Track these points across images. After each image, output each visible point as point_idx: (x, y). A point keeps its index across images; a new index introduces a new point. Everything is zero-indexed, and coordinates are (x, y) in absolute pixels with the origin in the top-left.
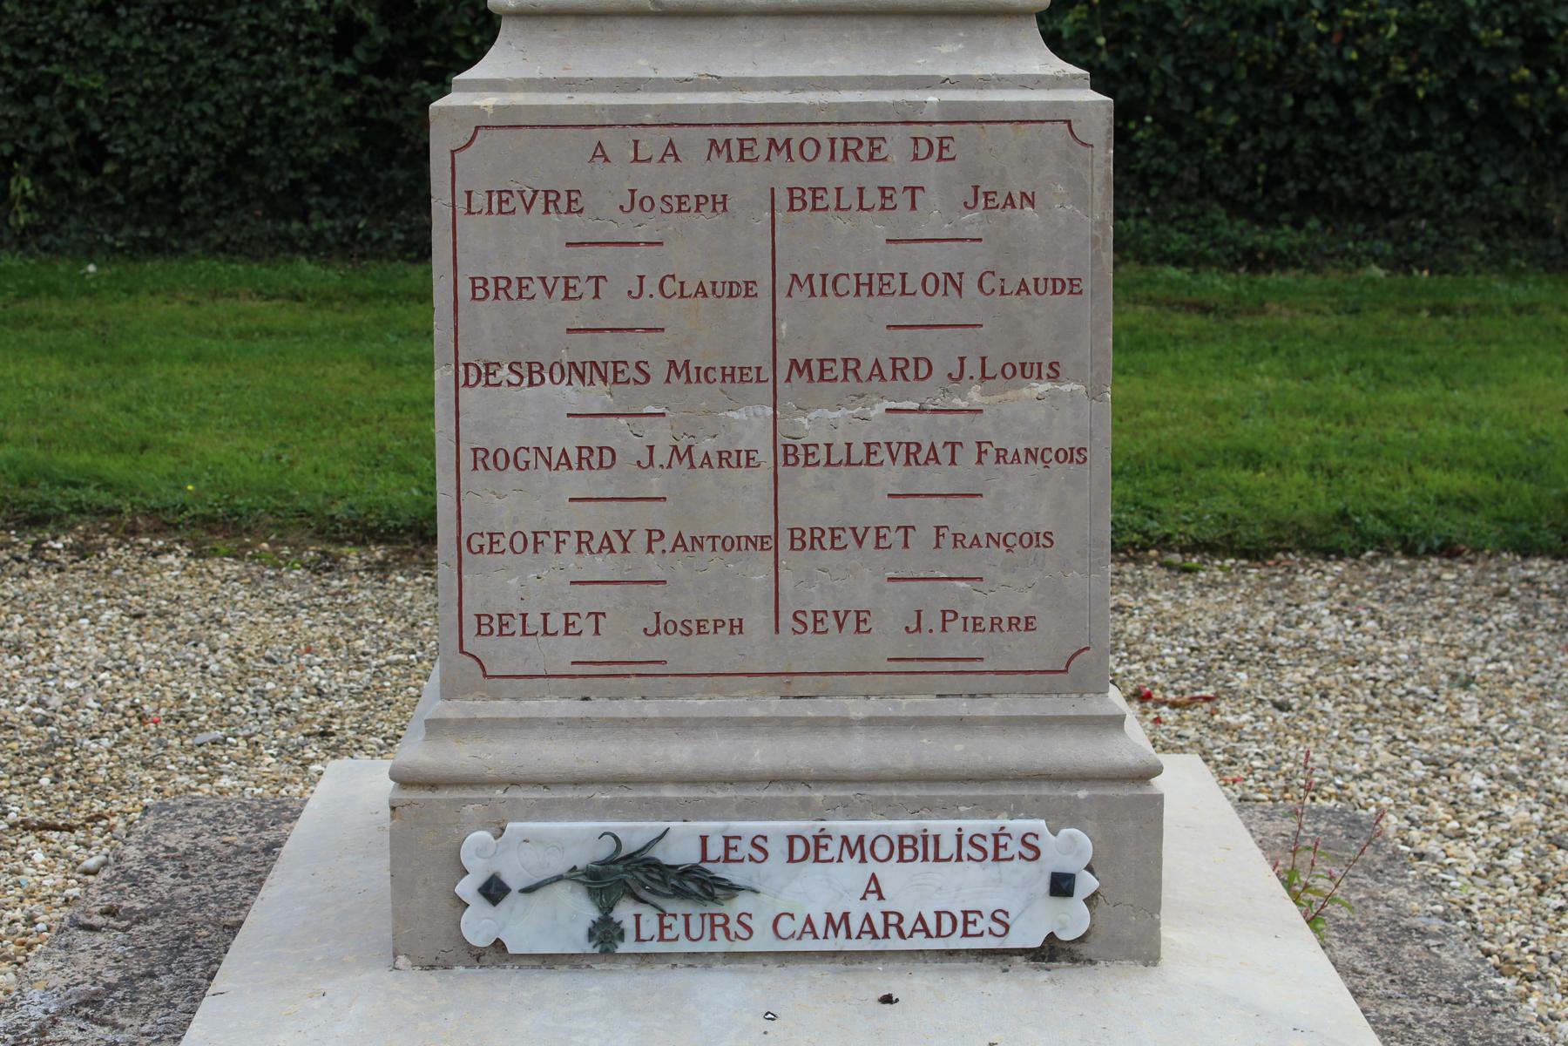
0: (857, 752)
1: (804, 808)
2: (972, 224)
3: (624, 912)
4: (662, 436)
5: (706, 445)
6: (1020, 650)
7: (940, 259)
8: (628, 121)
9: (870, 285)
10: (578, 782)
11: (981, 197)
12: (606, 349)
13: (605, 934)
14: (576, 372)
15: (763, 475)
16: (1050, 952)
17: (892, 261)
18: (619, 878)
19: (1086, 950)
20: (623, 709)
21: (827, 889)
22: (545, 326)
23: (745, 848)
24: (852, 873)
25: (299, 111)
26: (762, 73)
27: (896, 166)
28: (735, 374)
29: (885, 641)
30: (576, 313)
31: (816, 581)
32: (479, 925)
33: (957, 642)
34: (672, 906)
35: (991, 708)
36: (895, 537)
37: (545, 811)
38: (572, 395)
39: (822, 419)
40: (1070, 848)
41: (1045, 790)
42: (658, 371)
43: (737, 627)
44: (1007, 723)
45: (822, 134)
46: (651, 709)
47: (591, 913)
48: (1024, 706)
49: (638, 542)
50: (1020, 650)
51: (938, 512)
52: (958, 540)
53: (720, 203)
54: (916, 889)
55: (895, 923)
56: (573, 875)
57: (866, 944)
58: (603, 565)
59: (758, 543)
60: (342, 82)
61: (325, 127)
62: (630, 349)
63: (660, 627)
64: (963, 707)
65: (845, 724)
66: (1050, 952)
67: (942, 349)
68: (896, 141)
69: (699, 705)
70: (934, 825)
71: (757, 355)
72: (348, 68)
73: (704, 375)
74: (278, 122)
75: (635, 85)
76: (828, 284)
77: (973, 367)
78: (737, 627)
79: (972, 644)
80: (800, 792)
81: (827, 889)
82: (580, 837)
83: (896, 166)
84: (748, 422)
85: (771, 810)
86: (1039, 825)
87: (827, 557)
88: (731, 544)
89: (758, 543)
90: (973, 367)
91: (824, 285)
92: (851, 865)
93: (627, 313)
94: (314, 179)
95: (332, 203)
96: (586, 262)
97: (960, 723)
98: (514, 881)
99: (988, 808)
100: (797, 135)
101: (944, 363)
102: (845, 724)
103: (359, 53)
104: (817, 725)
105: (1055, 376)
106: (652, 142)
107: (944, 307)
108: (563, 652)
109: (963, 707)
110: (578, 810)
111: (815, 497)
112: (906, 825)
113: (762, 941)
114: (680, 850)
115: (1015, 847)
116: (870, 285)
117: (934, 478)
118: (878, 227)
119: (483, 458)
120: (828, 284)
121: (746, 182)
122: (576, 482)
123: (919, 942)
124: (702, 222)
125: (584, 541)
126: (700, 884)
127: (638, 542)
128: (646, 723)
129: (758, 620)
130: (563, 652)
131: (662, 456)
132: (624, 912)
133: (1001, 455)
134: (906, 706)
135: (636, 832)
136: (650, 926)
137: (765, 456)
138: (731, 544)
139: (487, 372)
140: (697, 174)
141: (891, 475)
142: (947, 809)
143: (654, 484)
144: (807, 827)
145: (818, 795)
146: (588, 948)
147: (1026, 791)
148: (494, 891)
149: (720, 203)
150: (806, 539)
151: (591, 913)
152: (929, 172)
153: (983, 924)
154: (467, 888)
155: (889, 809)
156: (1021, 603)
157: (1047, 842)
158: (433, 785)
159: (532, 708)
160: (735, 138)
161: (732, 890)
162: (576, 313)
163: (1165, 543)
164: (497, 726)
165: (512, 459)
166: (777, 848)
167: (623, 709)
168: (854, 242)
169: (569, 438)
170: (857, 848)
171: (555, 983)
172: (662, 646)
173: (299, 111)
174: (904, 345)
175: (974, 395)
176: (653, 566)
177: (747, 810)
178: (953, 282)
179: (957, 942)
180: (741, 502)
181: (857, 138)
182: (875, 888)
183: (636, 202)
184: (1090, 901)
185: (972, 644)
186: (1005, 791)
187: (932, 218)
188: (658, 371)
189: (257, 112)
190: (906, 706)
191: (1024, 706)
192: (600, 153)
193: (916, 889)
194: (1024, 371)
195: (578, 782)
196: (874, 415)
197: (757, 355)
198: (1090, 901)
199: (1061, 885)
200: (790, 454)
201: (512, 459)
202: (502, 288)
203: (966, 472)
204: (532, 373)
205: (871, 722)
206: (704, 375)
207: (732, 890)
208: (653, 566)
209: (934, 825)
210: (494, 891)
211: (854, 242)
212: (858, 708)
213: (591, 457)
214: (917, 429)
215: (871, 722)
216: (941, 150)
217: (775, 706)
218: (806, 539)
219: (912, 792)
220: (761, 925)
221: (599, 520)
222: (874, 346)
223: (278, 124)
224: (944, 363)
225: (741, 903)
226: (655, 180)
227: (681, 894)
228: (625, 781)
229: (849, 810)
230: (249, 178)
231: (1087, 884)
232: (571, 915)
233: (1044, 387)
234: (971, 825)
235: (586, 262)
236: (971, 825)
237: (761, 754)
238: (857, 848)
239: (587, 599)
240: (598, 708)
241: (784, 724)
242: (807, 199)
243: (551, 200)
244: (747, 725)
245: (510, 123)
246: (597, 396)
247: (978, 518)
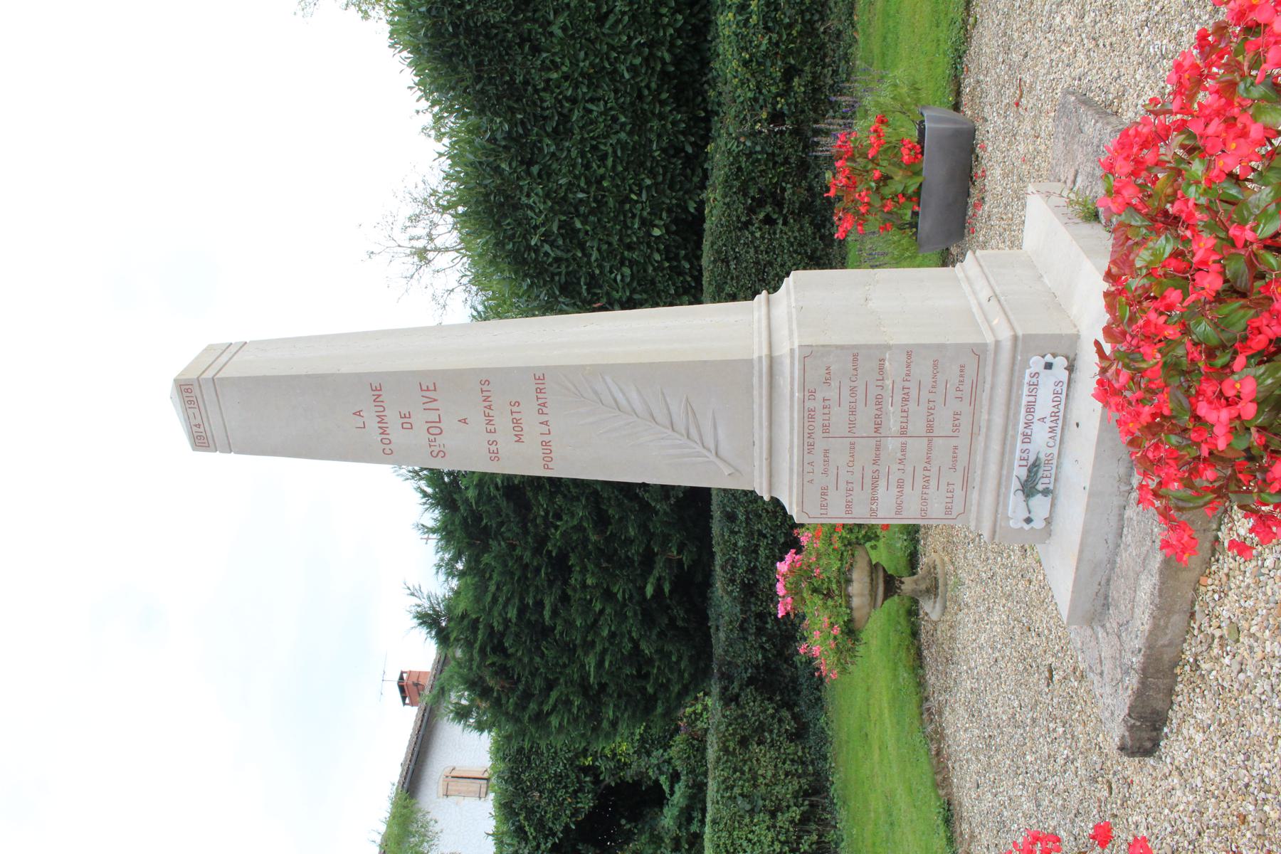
0: (998, 420)
1: (1014, 437)
2: (834, 384)
3: (1040, 487)
4: (895, 467)
5: (899, 455)
6: (970, 372)
7: (846, 392)
8: (802, 474)
9: (853, 412)
10: (998, 496)
11: (827, 382)
12: (868, 481)
13: (1046, 492)
14: (874, 487)
15: (909, 440)
16: (1071, 368)
17: (846, 406)
18: (1029, 489)
19: (1071, 356)
20: (978, 479)
21: (1041, 434)
23: (1025, 455)
24: (1037, 426)
25: (795, 238)
26: (788, 437)
27: (817, 404)
28: (878, 448)
29: (965, 408)
30: (857, 488)
31: (943, 423)
32: (1038, 524)
33: (967, 387)
34: (1040, 475)
35: (989, 379)
36: (931, 405)
37: (1006, 505)
38: (881, 489)
40: (1036, 363)
41: (1017, 368)
42: (875, 467)
43: (956, 448)
44: (994, 374)
45: (807, 424)
46: (979, 472)
47: (1039, 496)
48: (989, 369)
49: (927, 473)
50: (970, 372)
51: (924, 393)
52: (933, 387)
53: (826, 451)
54: (1044, 406)
55: (1054, 414)
56: (1026, 501)
57: (1060, 422)
58: (933, 483)
59: (930, 442)
60: (785, 223)
61: (801, 229)
62: (868, 474)
64: (988, 386)
65: (989, 421)
66: (1071, 368)
67: (873, 391)
68: (809, 404)
69: (979, 458)
70: (1024, 402)
71: (873, 441)
72: (780, 222)
73: (877, 456)
74: (800, 245)
75: (791, 470)
76: (852, 424)
77: (879, 383)
78: (956, 448)
79: (968, 382)
80: (1009, 437)
81: (1041, 434)
82: (1015, 501)
83: (817, 404)
84: (892, 445)
85: (1014, 446)
86: (1028, 372)
87: (936, 423)
88: (930, 449)
89: (930, 442)
90: (879, 383)
92: (1033, 426)
93: (858, 475)
94: (819, 230)
95: (828, 225)
96: (842, 485)
97: (992, 388)
98: (1027, 515)
99: (1020, 385)
100: (807, 431)
102: (989, 421)
103: (775, 216)
104: (988, 428)
105: (883, 360)
106: (808, 468)
108: (959, 493)
109: (988, 386)
110: (1007, 496)
111: (917, 425)
112: (1023, 411)
113: (1055, 451)
114: (1023, 473)
115: (1034, 380)
116: (853, 412)
117: (914, 393)
118: (835, 409)
120: (852, 424)
121: (820, 445)
122: (908, 489)
123: (1062, 407)
125: (925, 487)
126: (1034, 468)
127: (927, 473)
128: (983, 474)
129: (954, 442)
130: (959, 493)
131: (901, 467)
132: (1040, 487)
133: (908, 375)
134: (985, 402)
135: (1015, 485)
136: (1046, 480)
137: (903, 440)
138: (930, 449)
140: (818, 457)
141: (912, 406)
142: (1019, 397)
143: (909, 469)
144: (1020, 438)
145: (1010, 433)
146: (1050, 497)
147: (1016, 374)
149: (826, 451)
150: (930, 428)
151: (1039, 496)
152: (819, 396)
153: (1058, 388)
154: (1027, 527)
155: (1017, 413)
156: (956, 369)
157: (1033, 370)
158: (994, 532)
159: (975, 502)
160: (808, 446)
161: (1037, 459)
162: (857, 488)
163: (965, 22)
164: (979, 512)
165: (899, 505)
166: (1026, 446)
167: (978, 479)
168: (839, 417)
169: (894, 490)
170: (1028, 424)
171: (1060, 509)
172: (960, 467)
173: (795, 238)
175: (888, 382)
176: (935, 469)
177: (1012, 452)
178: (853, 389)
179: (1064, 396)
180: (917, 448)
181: (808, 415)
182: (1042, 419)
183: (825, 472)
184: (1054, 356)
185: (968, 382)
186: (1016, 380)
187: (833, 395)
188: (875, 467)
189: (795, 251)
190: (985, 402)
191: (989, 369)
192: (811, 481)
193: (1044, 406)
194: (881, 369)
195: (998, 496)
197: (873, 442)
198: (1054, 356)
199: (1049, 366)
200: (903, 433)
201: (899, 505)
202: (849, 506)
203: (913, 385)
204: (874, 500)
205: (989, 413)
206: (877, 456)
207: (1037, 459)
208: (935, 469)
209: (1024, 402)
210: (1028, 520)
211: (839, 417)
212: (985, 416)
214: (898, 398)
215: (989, 413)
216: (813, 393)
217: (981, 438)
218: (930, 428)
219: (1013, 406)
220: (1049, 451)
221: (919, 482)
222: (872, 410)
223: (800, 245)
225: (1042, 456)
226: (819, 468)
227: (1036, 473)
228: (999, 484)
229: (1016, 424)
230: (818, 253)
231: (1049, 358)
232: (1040, 505)
233: (887, 363)
234: (1025, 392)
235: (842, 485)
236: (1025, 392)
237: (995, 446)
238: (1028, 424)
239: (943, 487)
240: (977, 484)
241: (987, 437)
242: (826, 428)
243: (824, 494)
244: (987, 447)
245: (802, 503)
246: (882, 483)
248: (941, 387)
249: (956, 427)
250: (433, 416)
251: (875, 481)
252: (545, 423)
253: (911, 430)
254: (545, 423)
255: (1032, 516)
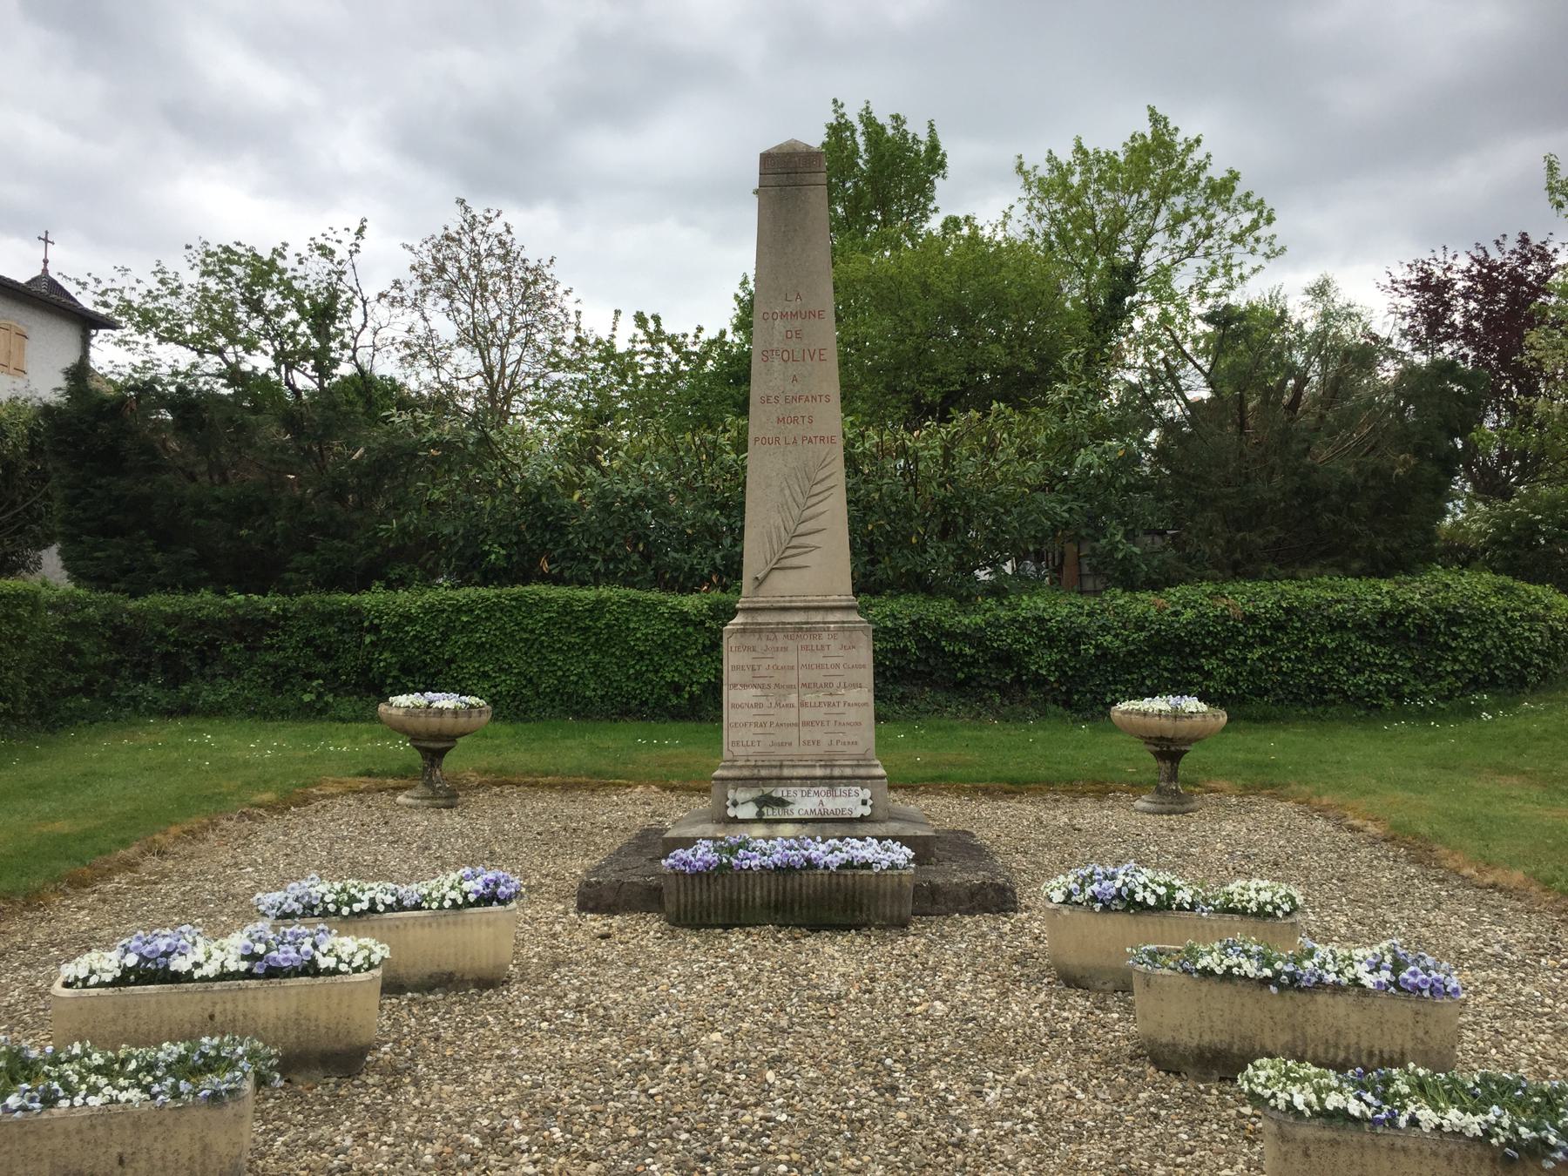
9: (819, 666)
12: (760, 681)
13: (760, 813)
17: (823, 661)
22: (747, 676)
28: (790, 687)
32: (731, 812)
38: (753, 691)
39: (809, 697)
58: (759, 730)
63: (773, 744)
67: (836, 681)
71: (795, 682)
76: (810, 667)
82: (755, 793)
88: (789, 725)
91: (810, 667)
101: (836, 683)
107: (837, 672)
111: (807, 714)
113: (796, 816)
116: (819, 666)
117: (835, 710)
119: (733, 706)
122: (755, 711)
124: (781, 654)
139: (735, 686)
141: (824, 709)
148: (735, 804)
149: (786, 649)
152: (831, 642)
156: (854, 739)
161: (789, 803)
169: (753, 701)
174: (828, 680)
178: (837, 666)
180: (792, 716)
196: (822, 697)
197: (795, 682)
199: (864, 803)
200: (803, 704)
203: (841, 709)
204: (745, 686)
207: (789, 803)
213: (757, 705)
214: (829, 699)
218: (805, 724)
221: (759, 719)
224: (836, 683)
239: (756, 738)
246: (759, 692)
247: (845, 719)
248: (842, 729)
249: (807, 743)
250: (798, 355)
251: (761, 687)
252: (795, 442)
253: (804, 711)
254: (795, 442)
255: (740, 807)
